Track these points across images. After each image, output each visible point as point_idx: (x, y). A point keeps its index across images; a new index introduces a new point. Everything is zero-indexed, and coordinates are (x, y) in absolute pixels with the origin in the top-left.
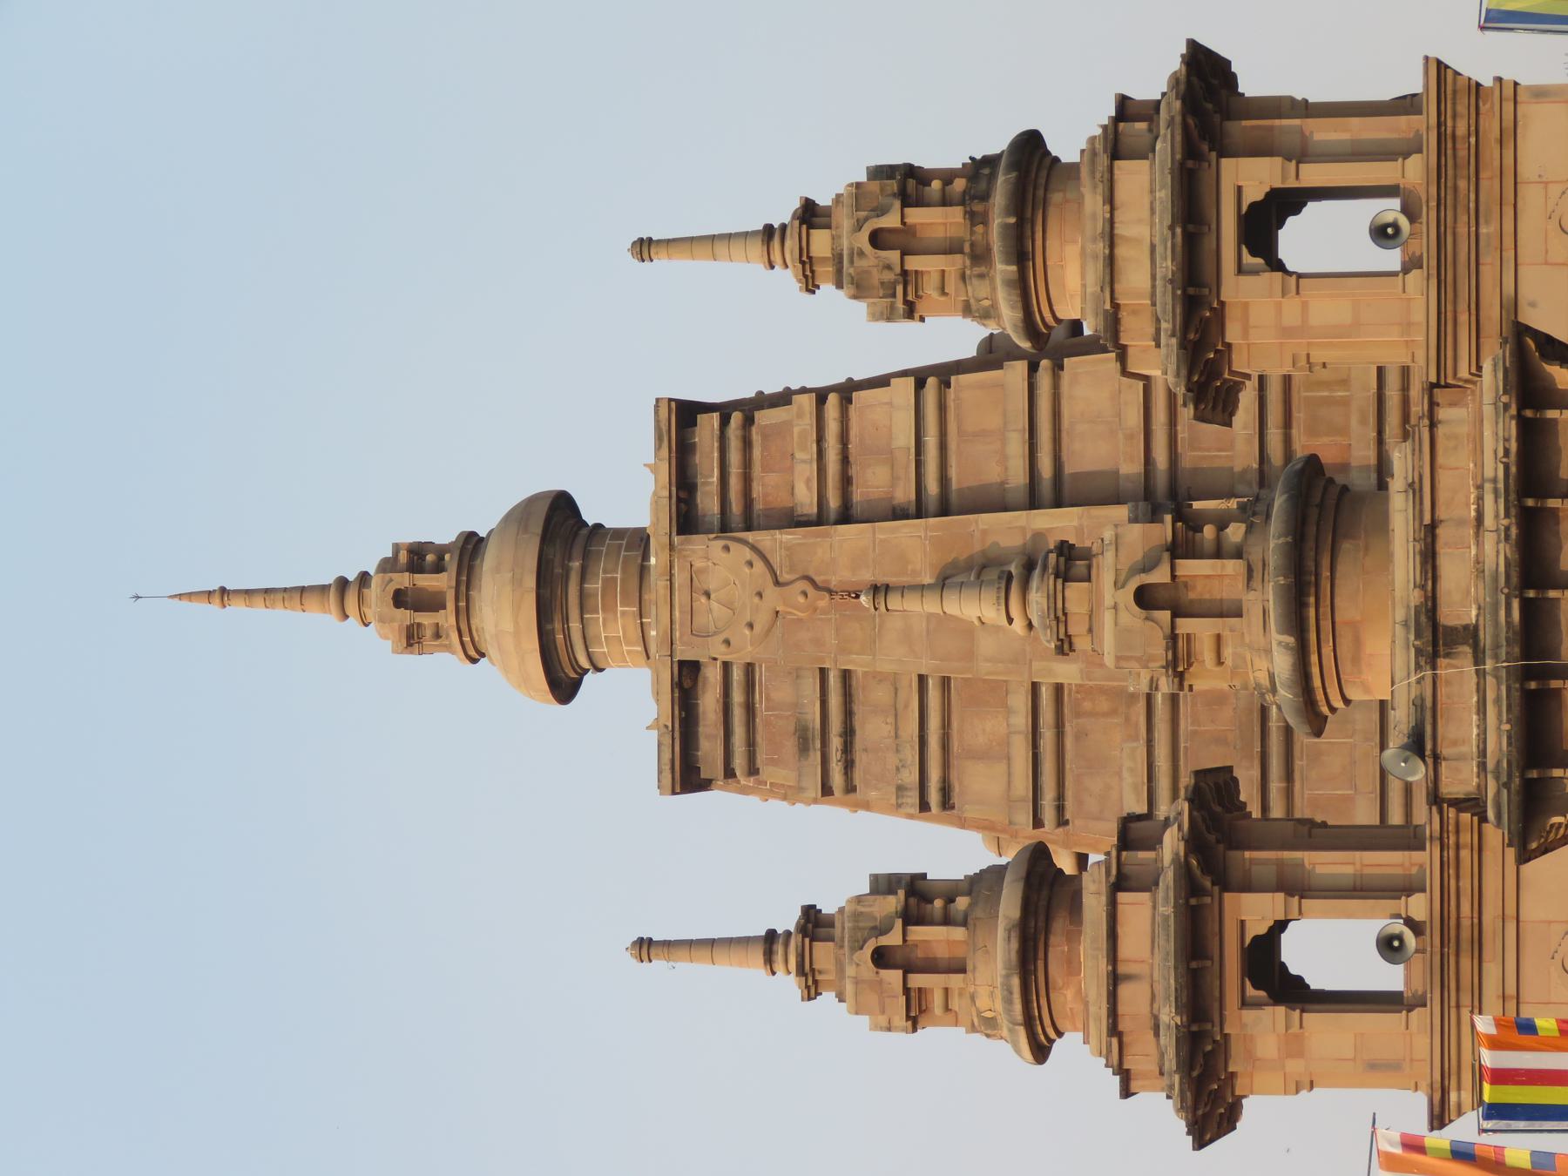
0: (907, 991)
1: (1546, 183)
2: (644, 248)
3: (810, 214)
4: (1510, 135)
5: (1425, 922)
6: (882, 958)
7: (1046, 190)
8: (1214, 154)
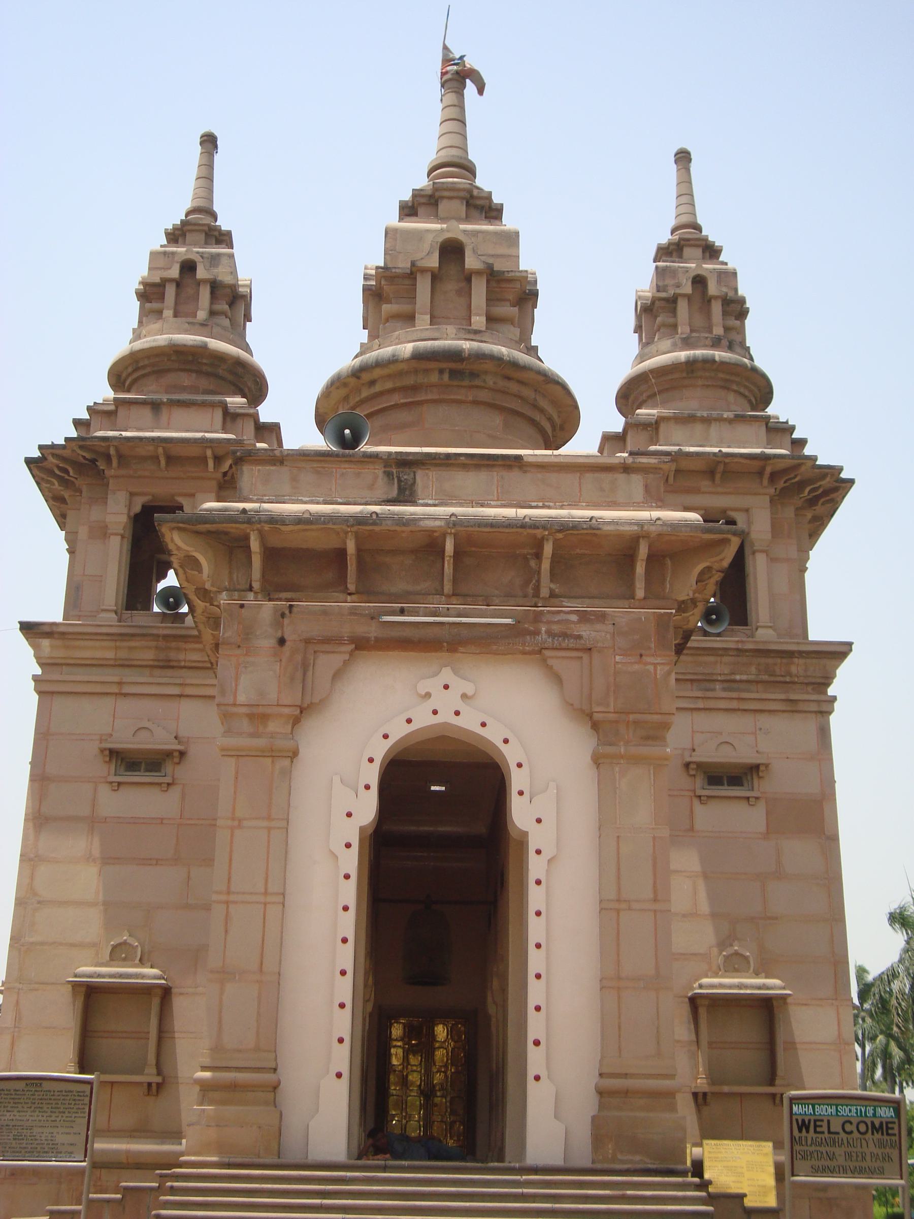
0: (164, 282)
1: (755, 734)
2: (683, 158)
3: (711, 251)
4: (793, 708)
5: (183, 622)
6: (188, 267)
7: (735, 391)
8: (772, 491)
